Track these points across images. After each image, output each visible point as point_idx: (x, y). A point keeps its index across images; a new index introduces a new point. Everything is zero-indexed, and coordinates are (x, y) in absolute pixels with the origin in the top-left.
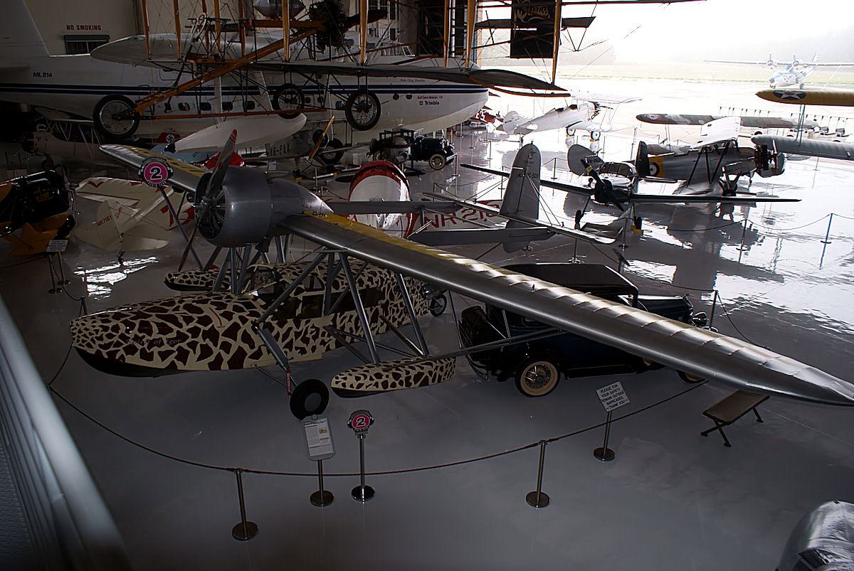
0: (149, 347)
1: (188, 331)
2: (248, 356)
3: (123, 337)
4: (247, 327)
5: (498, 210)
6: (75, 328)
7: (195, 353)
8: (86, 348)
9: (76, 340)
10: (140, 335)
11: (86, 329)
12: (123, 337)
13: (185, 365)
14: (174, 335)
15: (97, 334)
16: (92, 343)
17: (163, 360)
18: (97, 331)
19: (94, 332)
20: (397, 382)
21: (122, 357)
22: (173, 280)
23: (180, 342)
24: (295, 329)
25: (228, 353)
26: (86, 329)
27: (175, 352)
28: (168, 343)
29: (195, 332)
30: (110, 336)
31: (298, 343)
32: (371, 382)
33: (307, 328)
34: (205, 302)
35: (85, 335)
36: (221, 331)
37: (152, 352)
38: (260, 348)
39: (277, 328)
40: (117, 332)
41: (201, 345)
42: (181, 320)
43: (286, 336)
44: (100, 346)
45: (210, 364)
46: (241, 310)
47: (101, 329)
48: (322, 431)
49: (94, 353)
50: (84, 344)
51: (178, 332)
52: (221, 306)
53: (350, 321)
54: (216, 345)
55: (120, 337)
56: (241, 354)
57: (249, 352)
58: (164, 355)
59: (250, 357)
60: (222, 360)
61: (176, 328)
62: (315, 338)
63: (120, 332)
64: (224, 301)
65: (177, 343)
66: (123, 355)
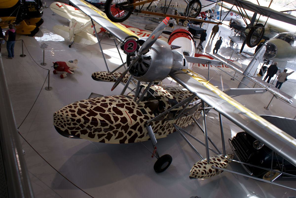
0: (94, 132)
2: (138, 137)
4: (142, 124)
5: (242, 72)
6: (56, 117)
7: (115, 136)
8: (60, 127)
10: (91, 126)
11: (63, 119)
12: (82, 126)
13: (109, 141)
15: (68, 122)
16: (64, 125)
17: (99, 138)
19: (67, 121)
22: (96, 76)
23: (110, 131)
25: (130, 135)
27: (106, 135)
29: (118, 126)
30: (75, 124)
31: (160, 131)
34: (122, 106)
36: (130, 126)
42: (112, 119)
44: (68, 128)
46: (140, 115)
47: (70, 120)
49: (64, 131)
51: (110, 126)
52: (131, 111)
53: (182, 121)
54: (126, 132)
55: (80, 125)
58: (100, 136)
62: (167, 129)
63: (81, 123)
64: (131, 106)
65: (108, 131)
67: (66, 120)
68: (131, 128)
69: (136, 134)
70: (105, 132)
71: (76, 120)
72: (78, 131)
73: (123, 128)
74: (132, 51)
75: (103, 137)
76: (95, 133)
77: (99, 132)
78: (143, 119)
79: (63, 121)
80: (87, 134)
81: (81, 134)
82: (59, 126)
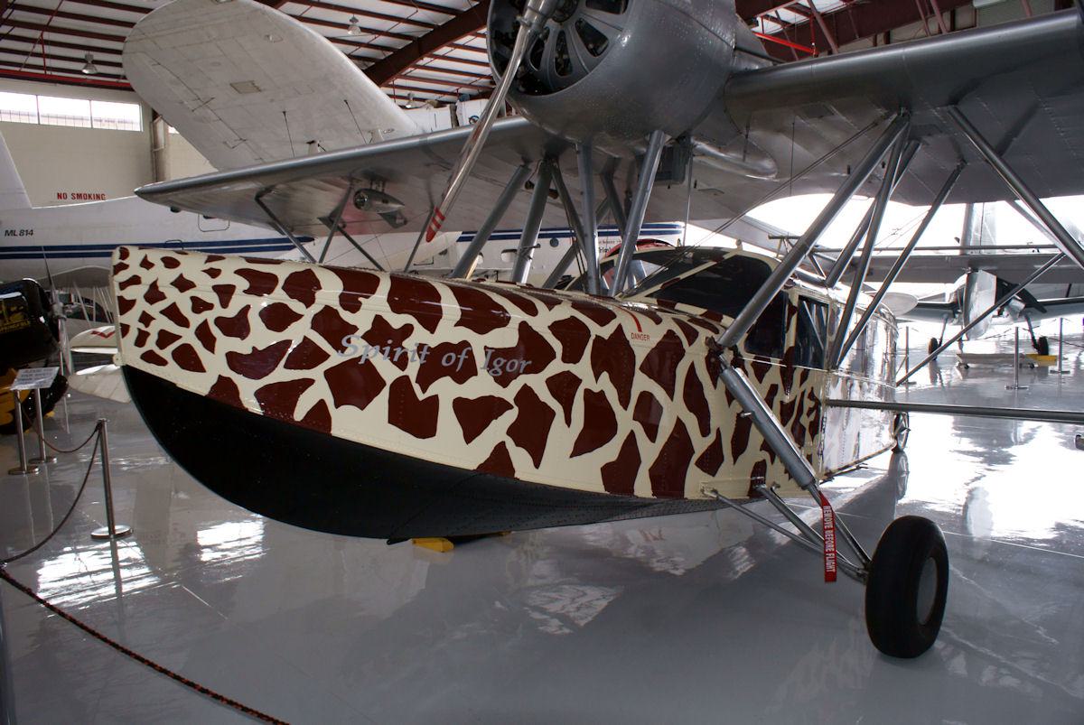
0: (426, 378)
3: (332, 326)
6: (135, 280)
7: (568, 421)
8: (172, 373)
10: (397, 321)
11: (183, 284)
13: (537, 465)
14: (506, 337)
15: (225, 304)
16: (198, 346)
18: (225, 293)
19: (213, 298)
21: (320, 409)
23: (528, 371)
26: (183, 284)
27: (512, 407)
28: (490, 366)
30: (278, 318)
33: (803, 394)
35: (173, 313)
36: (641, 351)
37: (435, 399)
40: (309, 302)
41: (588, 392)
44: (234, 360)
47: (242, 284)
50: (166, 354)
54: (625, 402)
57: (700, 444)
58: (474, 416)
60: (638, 461)
61: (517, 315)
66: (322, 404)
70: (497, 380)
71: (281, 283)
72: (308, 383)
76: (431, 391)
77: (460, 378)
79: (184, 302)
80: (381, 402)
81: (337, 405)
82: (161, 362)
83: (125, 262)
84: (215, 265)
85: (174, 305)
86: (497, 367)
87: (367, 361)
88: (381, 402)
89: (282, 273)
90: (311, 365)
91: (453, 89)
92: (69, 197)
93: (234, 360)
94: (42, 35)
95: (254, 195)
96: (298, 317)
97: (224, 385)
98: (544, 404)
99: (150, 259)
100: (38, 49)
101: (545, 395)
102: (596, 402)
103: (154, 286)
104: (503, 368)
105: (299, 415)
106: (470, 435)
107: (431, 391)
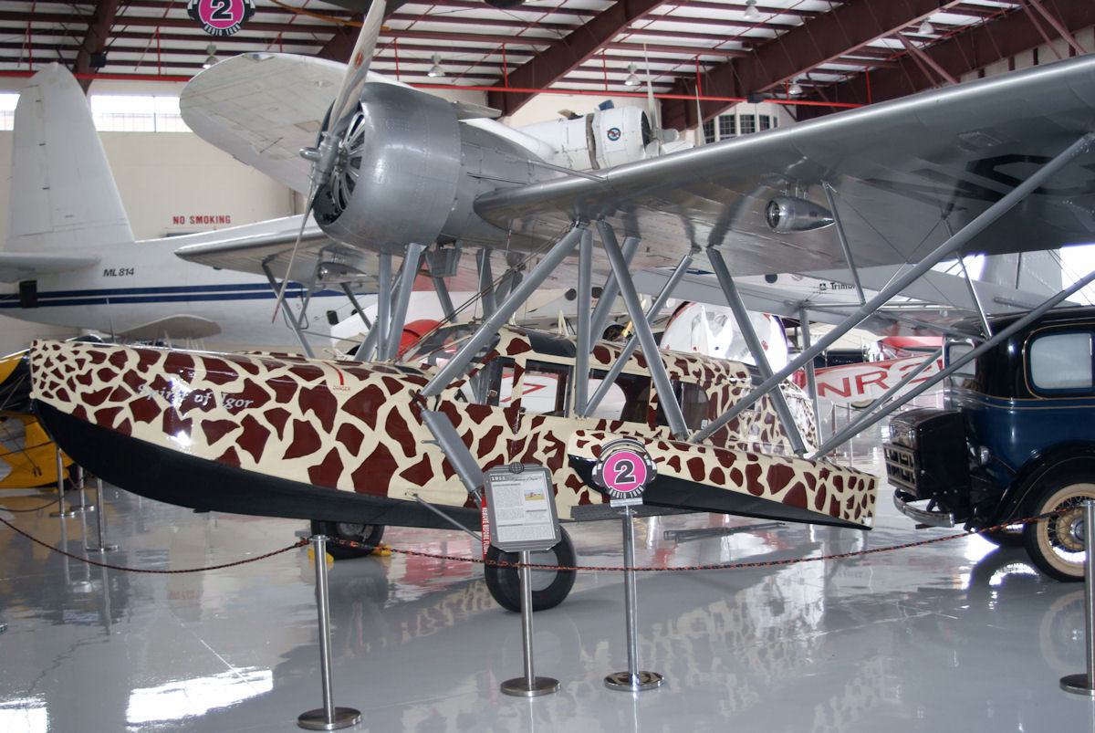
1: (269, 382)
4: (400, 401)
6: (40, 356)
7: (281, 437)
8: (56, 402)
9: (38, 383)
11: (61, 358)
13: (257, 460)
14: (237, 387)
15: (80, 368)
17: (211, 442)
18: (81, 363)
19: (75, 365)
20: (727, 472)
23: (250, 406)
24: (507, 433)
25: (354, 451)
26: (61, 358)
27: (237, 426)
28: (225, 403)
30: (106, 375)
32: (662, 453)
33: (536, 436)
35: (56, 372)
36: (342, 399)
38: (426, 456)
39: (467, 423)
40: (121, 367)
41: (296, 422)
43: (487, 443)
44: (85, 396)
45: (313, 471)
47: (89, 358)
48: (531, 496)
50: (53, 393)
51: (247, 381)
54: (328, 428)
56: (380, 464)
57: (404, 463)
59: (405, 475)
60: (340, 467)
61: (243, 374)
65: (241, 408)
67: (71, 362)
68: (346, 408)
69: (381, 450)
70: (229, 411)
71: (108, 357)
72: (120, 409)
73: (308, 400)
74: (231, 23)
75: (227, 435)
77: (206, 409)
78: (403, 382)
79: (62, 367)
80: (159, 420)
81: (136, 420)
82: (51, 397)
83: (36, 347)
84: (77, 348)
85: (57, 369)
86: (229, 404)
87: (152, 399)
88: (159, 420)
89: (109, 352)
90: (122, 399)
91: (691, 56)
92: (188, 220)
93: (85, 396)
94: (157, 30)
95: (261, 262)
96: (116, 375)
97: (80, 409)
98: (262, 426)
99: (47, 346)
100: (154, 43)
101: (263, 421)
102: (303, 430)
103: (48, 359)
104: (233, 404)
105: (116, 424)
106: (211, 440)
107: (187, 415)
